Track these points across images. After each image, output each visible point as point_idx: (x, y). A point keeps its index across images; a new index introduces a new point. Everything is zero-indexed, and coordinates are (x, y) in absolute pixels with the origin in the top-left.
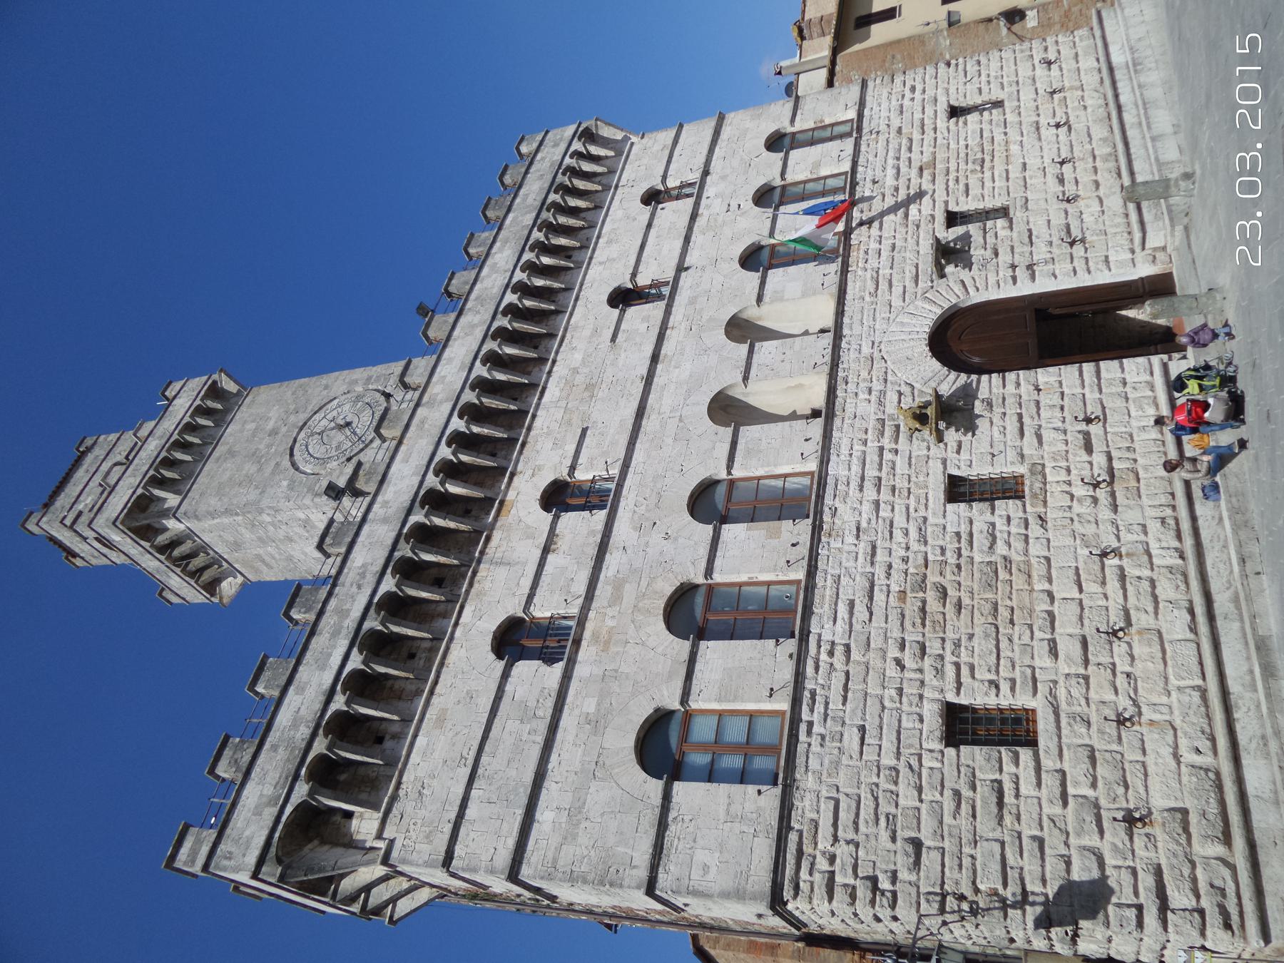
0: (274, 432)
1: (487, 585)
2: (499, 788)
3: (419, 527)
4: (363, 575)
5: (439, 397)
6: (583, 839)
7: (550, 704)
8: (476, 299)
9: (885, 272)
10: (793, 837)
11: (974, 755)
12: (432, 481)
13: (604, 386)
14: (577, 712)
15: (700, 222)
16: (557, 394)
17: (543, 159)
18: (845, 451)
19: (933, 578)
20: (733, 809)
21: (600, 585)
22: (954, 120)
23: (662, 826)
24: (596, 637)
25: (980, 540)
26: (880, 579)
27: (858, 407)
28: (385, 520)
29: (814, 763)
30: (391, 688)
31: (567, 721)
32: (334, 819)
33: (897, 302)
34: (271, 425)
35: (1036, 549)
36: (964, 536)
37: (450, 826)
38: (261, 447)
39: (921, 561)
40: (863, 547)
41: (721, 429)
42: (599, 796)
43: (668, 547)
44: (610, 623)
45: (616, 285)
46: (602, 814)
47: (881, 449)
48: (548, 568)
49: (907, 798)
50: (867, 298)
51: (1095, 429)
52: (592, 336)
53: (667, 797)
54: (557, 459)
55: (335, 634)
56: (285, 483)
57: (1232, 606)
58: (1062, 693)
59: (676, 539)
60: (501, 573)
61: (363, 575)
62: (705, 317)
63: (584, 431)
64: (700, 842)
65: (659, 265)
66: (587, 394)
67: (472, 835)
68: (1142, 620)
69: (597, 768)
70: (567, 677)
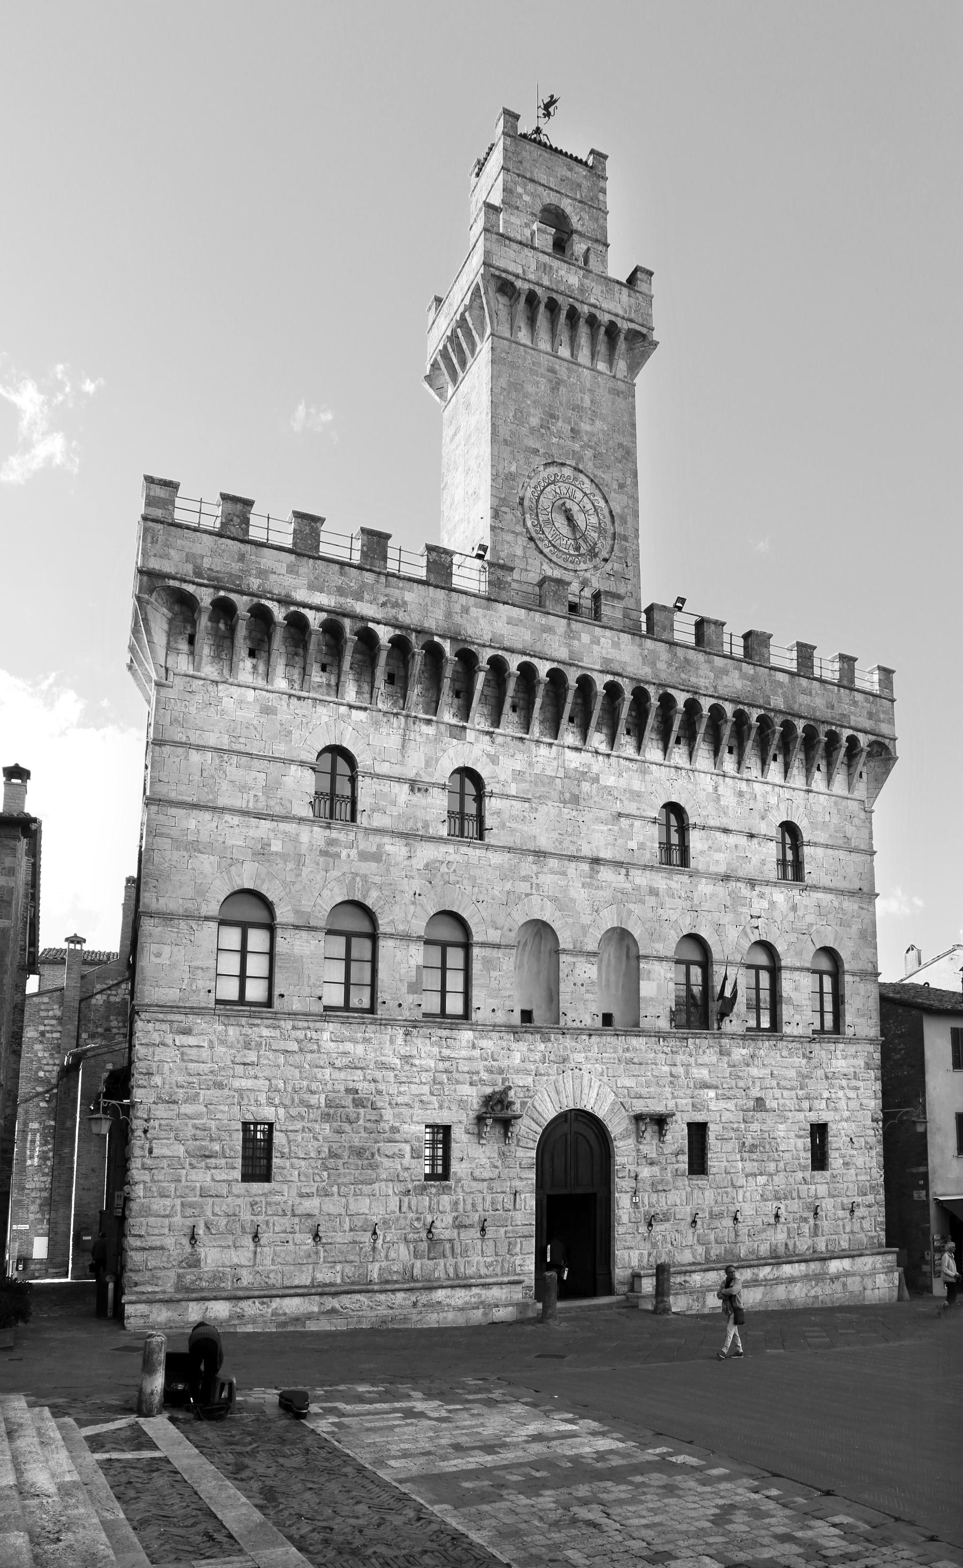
2: (213, 777)
6: (176, 855)
7: (278, 810)
10: (181, 1017)
13: (574, 813)
14: (272, 835)
15: (745, 890)
16: (573, 765)
18: (484, 1043)
20: (200, 972)
21: (377, 839)
22: (809, 1127)
23: (187, 917)
24: (331, 842)
29: (232, 1031)
30: (296, 654)
32: (189, 628)
34: (585, 427)
36: (397, 1137)
37: (184, 740)
38: (560, 424)
39: (379, 1104)
41: (513, 934)
42: (206, 863)
43: (408, 896)
44: (344, 854)
45: (687, 808)
46: (193, 869)
47: (478, 1073)
48: (396, 787)
50: (628, 1055)
51: (475, 1233)
52: (632, 792)
53: (207, 918)
54: (502, 778)
57: (330, 1308)
58: (278, 1198)
59: (414, 903)
60: (393, 741)
62: (631, 906)
63: (527, 800)
64: (176, 949)
65: (702, 852)
66: (567, 795)
67: (177, 760)
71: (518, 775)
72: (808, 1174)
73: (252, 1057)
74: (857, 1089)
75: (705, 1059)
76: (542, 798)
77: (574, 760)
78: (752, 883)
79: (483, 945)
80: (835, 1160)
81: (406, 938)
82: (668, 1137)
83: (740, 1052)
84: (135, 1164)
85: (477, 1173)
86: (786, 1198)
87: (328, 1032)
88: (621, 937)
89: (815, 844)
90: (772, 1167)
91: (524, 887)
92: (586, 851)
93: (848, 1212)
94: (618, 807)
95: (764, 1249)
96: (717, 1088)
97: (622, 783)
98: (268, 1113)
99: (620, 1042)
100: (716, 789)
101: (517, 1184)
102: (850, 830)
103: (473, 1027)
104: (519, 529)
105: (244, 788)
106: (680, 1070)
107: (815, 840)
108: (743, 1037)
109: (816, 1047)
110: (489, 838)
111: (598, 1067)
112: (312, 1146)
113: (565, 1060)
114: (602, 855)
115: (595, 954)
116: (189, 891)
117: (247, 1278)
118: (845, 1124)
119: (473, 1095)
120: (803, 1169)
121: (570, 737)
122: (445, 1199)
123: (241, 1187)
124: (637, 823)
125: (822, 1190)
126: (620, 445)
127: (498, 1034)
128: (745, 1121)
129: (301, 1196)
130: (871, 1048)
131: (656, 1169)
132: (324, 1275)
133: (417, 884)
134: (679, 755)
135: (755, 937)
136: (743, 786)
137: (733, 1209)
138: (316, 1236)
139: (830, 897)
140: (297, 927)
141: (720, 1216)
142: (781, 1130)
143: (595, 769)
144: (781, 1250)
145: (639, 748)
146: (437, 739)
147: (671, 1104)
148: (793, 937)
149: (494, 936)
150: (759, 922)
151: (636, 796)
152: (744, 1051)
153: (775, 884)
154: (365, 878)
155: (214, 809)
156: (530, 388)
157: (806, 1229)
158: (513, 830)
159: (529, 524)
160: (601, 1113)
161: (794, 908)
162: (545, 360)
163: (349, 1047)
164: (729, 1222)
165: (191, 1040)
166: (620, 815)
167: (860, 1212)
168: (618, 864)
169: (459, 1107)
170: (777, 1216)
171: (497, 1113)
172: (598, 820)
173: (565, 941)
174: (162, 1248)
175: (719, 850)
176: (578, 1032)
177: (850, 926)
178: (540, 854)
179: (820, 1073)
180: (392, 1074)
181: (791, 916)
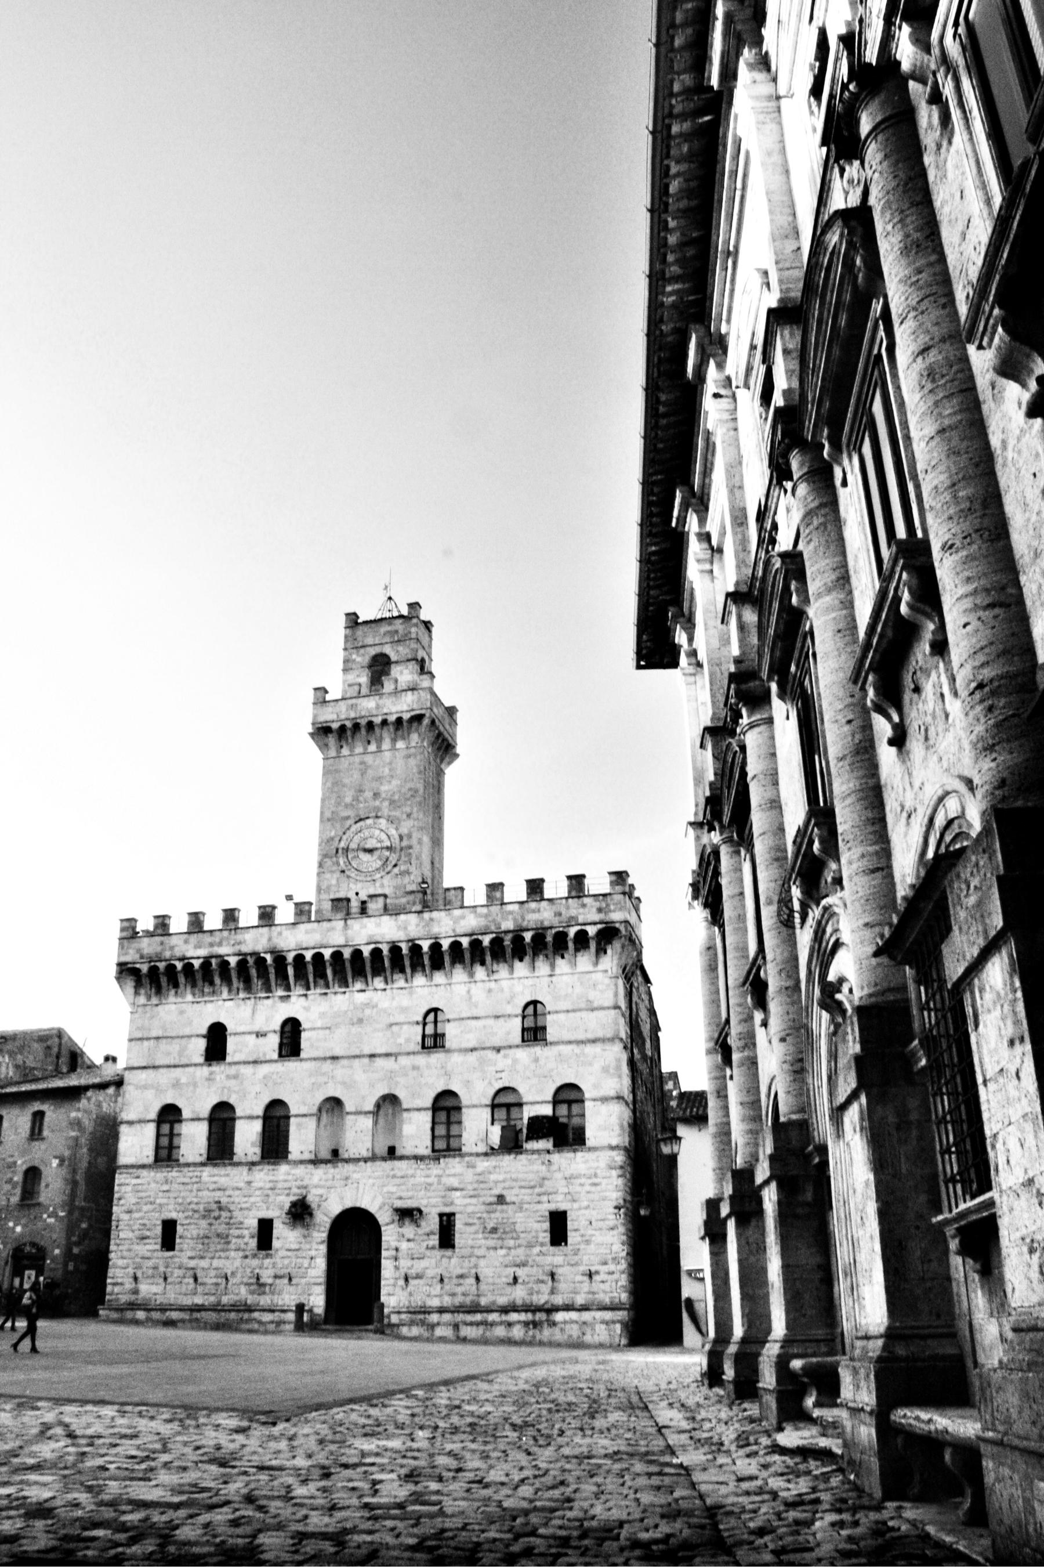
0: (376, 795)
1: (243, 1007)
3: (265, 960)
4: (240, 943)
5: (349, 932)
7: (184, 1061)
8: (432, 920)
9: (412, 1181)
11: (159, 1230)
12: (290, 957)
15: (491, 1055)
17: (584, 906)
18: (293, 1172)
19: (224, 1214)
21: (237, 1067)
23: (140, 1121)
25: (237, 1232)
26: (227, 1193)
27: (318, 1175)
28: (270, 939)
31: (179, 1070)
33: (385, 1190)
34: (384, 788)
35: (233, 1254)
40: (242, 1185)
42: (150, 1094)
43: (253, 1094)
44: (218, 1078)
49: (145, 1208)
51: (286, 1281)
55: (211, 945)
56: (333, 834)
61: (240, 943)
65: (456, 1036)
68: (200, 1289)
69: (159, 1090)
70: (195, 1065)
71: (322, 1015)
72: (544, 1249)
73: (165, 1187)
74: (595, 1185)
75: (453, 1171)
76: (337, 1025)
77: (360, 998)
78: (498, 1050)
79: (296, 1116)
80: (572, 1237)
81: (251, 1118)
82: (423, 1223)
83: (483, 1164)
84: (112, 1242)
85: (287, 1246)
86: (524, 1264)
87: (208, 1171)
88: (390, 1101)
89: (557, 1012)
90: (511, 1243)
91: (322, 1079)
92: (367, 1051)
93: (586, 1278)
94: (392, 1020)
95: (502, 1301)
96: (462, 1190)
97: (395, 1004)
98: (173, 1215)
99: (389, 1165)
100: (469, 992)
101: (313, 1253)
102: (592, 995)
103: (289, 1163)
104: (335, 868)
105: (169, 1054)
106: (435, 1180)
107: (558, 1008)
108: (486, 1154)
109: (556, 1157)
110: (303, 1055)
111: (371, 1181)
112: (195, 1233)
113: (347, 1178)
114: (379, 1051)
115: (369, 1112)
116: (141, 1109)
117: (160, 1299)
118: (583, 1212)
119: (286, 1202)
120: (542, 1245)
121: (359, 985)
122: (267, 1261)
123: (160, 1254)
124: (405, 1027)
125: (559, 1260)
126: (410, 789)
127: (302, 1167)
128: (488, 1212)
129: (191, 1258)
130: (614, 1153)
131: (411, 1245)
132: (198, 1300)
133: (258, 1088)
134: (439, 977)
135: (499, 1085)
136: (493, 985)
137: (473, 1271)
138: (196, 1279)
139: (570, 1047)
140: (193, 1120)
141: (461, 1276)
142: (519, 1218)
143: (375, 1000)
144: (519, 1302)
145: (406, 980)
146: (273, 1006)
147: (424, 1202)
148: (535, 1081)
149: (304, 1110)
150: (503, 1075)
151: (404, 1010)
152: (486, 1164)
153: (517, 1046)
154: (229, 1089)
155: (154, 1067)
156: (346, 781)
157: (546, 1288)
158: (317, 1049)
159: (341, 862)
160: (373, 1209)
161: (536, 1060)
162: (357, 759)
163: (215, 1179)
164: (473, 1281)
165: (138, 1181)
166: (391, 1025)
167: (596, 1278)
168: (388, 1055)
169: (276, 1210)
170: (515, 1279)
171: (300, 1212)
172: (375, 1030)
173: (349, 1106)
174: (122, 1284)
175: (470, 1031)
176: (358, 1160)
177: (591, 1064)
178: (334, 1058)
179: (558, 1175)
180: (237, 1192)
181: (533, 1066)
